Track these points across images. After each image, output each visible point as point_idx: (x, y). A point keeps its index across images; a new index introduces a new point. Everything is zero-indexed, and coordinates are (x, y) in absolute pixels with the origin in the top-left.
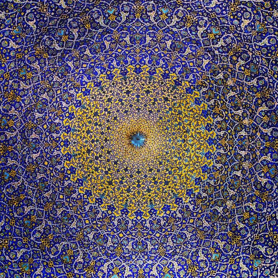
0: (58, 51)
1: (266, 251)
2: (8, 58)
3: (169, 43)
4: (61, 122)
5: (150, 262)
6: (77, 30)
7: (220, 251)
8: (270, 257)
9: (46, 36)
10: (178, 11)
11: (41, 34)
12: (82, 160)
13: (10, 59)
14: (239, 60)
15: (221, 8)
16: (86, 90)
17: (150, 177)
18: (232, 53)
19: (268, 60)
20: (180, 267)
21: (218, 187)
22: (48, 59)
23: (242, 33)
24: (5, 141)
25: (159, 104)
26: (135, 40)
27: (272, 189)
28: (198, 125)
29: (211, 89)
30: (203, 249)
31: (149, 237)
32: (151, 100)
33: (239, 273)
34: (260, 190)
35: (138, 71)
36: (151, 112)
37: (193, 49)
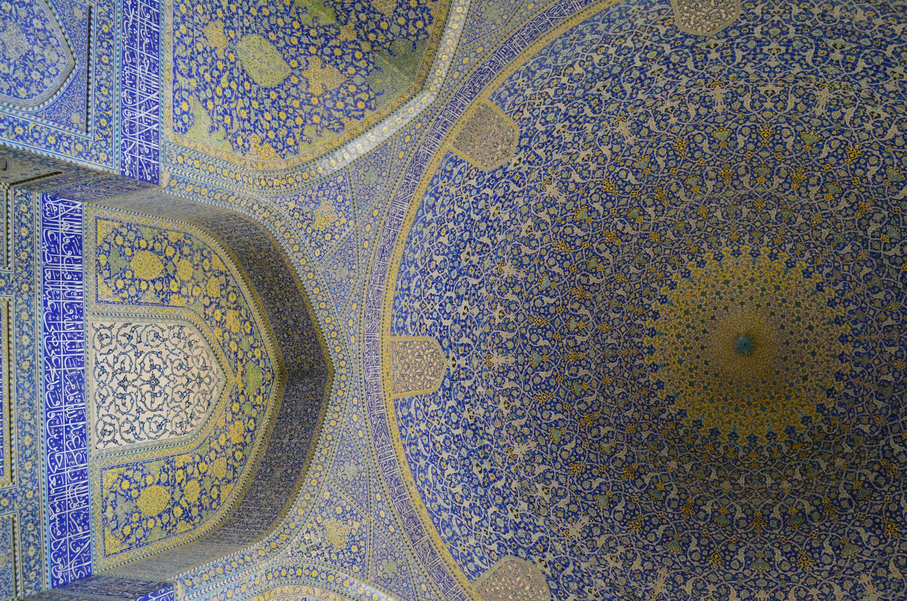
0: (865, 230)
1: (619, 511)
2: (853, 167)
3: (889, 378)
4: (765, 244)
5: (593, 367)
6: (899, 253)
8: (612, 516)
11: (889, 207)
12: (715, 274)
14: (875, 474)
16: (811, 273)
17: (698, 363)
18: (884, 463)
19: (880, 513)
21: (692, 449)
22: (854, 220)
25: (798, 369)
26: (889, 332)
27: (699, 519)
28: (773, 421)
30: (613, 433)
31: (623, 364)
32: (802, 358)
33: (589, 478)
34: (696, 504)
35: (843, 339)
36: (785, 359)
37: (884, 411)
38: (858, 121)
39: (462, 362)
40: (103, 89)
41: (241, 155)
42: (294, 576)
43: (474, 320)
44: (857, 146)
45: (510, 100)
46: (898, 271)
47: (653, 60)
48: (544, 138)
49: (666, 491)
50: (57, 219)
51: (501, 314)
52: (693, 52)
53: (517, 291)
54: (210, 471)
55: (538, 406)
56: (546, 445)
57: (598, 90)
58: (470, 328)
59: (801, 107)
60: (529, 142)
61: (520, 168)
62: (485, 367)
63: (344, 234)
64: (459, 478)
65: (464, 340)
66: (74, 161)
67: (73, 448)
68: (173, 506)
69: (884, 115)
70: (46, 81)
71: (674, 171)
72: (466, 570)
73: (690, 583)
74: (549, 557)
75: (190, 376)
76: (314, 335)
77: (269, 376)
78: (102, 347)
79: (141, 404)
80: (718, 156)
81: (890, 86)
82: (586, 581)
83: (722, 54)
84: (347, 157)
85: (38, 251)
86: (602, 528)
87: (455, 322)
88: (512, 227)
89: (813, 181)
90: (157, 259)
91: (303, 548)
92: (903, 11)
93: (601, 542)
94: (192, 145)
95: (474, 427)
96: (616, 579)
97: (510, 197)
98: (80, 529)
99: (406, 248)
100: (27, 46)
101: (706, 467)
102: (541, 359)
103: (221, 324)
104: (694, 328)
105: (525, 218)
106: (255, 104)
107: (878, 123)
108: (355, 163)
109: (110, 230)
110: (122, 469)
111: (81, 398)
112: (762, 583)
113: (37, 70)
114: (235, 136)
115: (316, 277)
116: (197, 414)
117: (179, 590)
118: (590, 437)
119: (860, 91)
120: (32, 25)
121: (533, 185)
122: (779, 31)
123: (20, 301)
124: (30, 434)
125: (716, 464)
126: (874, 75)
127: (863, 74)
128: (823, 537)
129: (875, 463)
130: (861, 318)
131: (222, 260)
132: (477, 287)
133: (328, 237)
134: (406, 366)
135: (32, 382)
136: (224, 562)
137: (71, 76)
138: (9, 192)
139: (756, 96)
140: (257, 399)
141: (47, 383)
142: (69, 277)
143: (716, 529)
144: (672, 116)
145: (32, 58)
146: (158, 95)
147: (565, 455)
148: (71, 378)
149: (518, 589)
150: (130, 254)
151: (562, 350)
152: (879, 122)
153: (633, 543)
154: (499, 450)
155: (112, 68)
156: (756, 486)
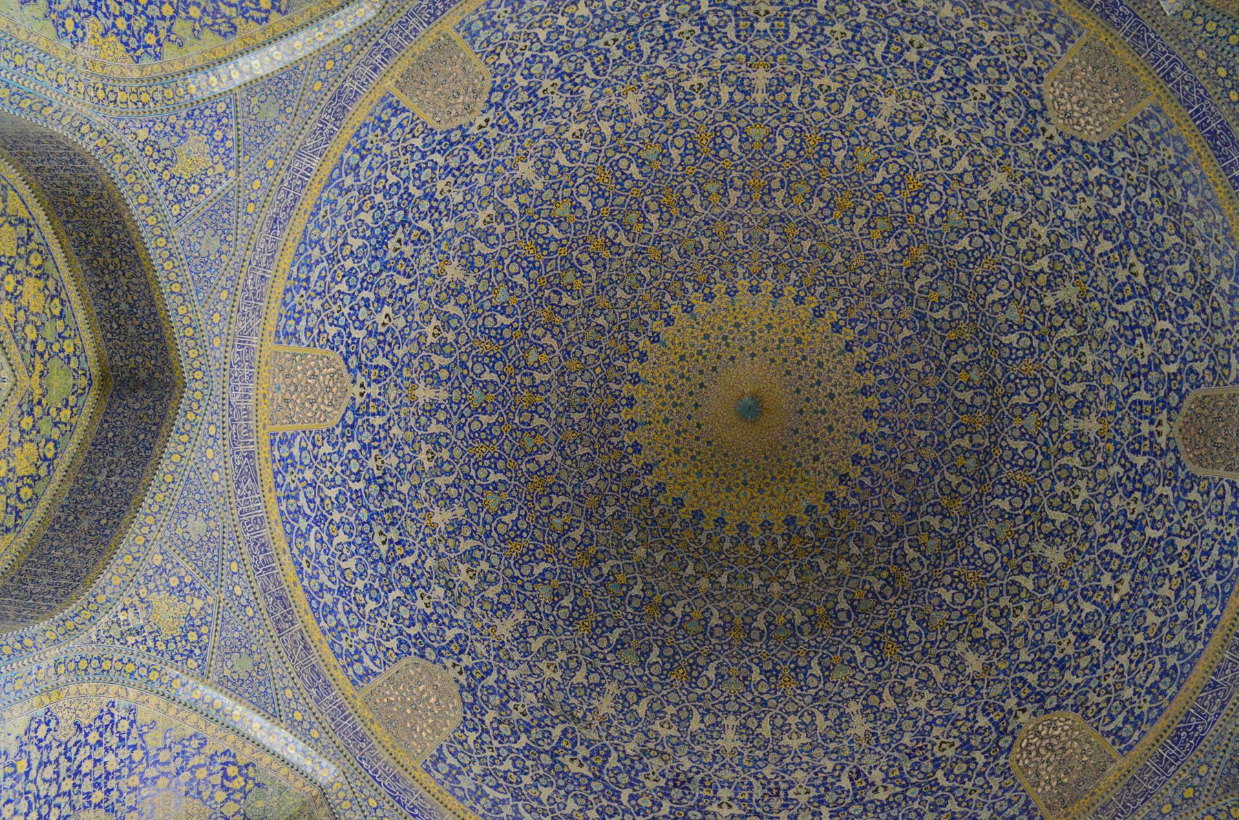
0: (912, 283)
2: (910, 201)
3: (914, 468)
4: (791, 282)
5: (553, 415)
6: (947, 317)
7: (565, 532)
9: (939, 265)
10: (969, 485)
11: (944, 258)
13: (908, 204)
14: (882, 582)
15: (972, 556)
19: (881, 630)
20: (543, 464)
23: (928, 590)
24: (770, 189)
26: (922, 411)
28: (771, 508)
29: (832, 533)
31: (593, 416)
32: (816, 433)
34: (663, 604)
35: (868, 414)
36: (796, 432)
37: (903, 508)
38: (924, 144)
39: (374, 390)
41: (69, 46)
42: (99, 671)
43: (397, 334)
44: (918, 176)
45: (484, 35)
46: (943, 338)
47: (684, 16)
48: (524, 97)
49: (628, 586)
51: (436, 331)
52: (736, 15)
53: (462, 303)
55: (473, 461)
56: (478, 514)
57: (606, 44)
58: (390, 344)
59: (860, 114)
60: (503, 99)
61: (486, 133)
62: (406, 401)
63: (219, 188)
64: (353, 548)
65: (381, 361)
69: (956, 142)
71: (690, 171)
72: (350, 672)
73: (644, 703)
74: (467, 660)
76: (159, 329)
77: (84, 382)
80: (749, 160)
81: (968, 107)
82: (512, 694)
83: (773, 25)
84: (235, 75)
86: (540, 627)
87: (370, 334)
88: (466, 213)
89: (860, 211)
91: (116, 631)
92: (997, 15)
93: (536, 645)
95: (381, 481)
96: (552, 693)
97: (468, 171)
101: (682, 558)
102: (484, 397)
104: (688, 379)
105: (485, 204)
107: (948, 151)
108: (248, 87)
112: (732, 707)
114: (63, 15)
115: (170, 246)
118: (537, 508)
119: (932, 106)
121: (501, 158)
122: (847, 9)
125: (696, 555)
126: (952, 89)
127: (939, 85)
128: (812, 654)
129: (883, 569)
130: (892, 391)
131: (23, 199)
132: (406, 289)
133: (194, 189)
134: (292, 388)
139: (806, 90)
140: (62, 414)
143: (684, 637)
144: (697, 96)
147: (502, 529)
149: (420, 701)
151: (513, 389)
152: (948, 149)
153: (579, 649)
154: (413, 516)
156: (740, 587)
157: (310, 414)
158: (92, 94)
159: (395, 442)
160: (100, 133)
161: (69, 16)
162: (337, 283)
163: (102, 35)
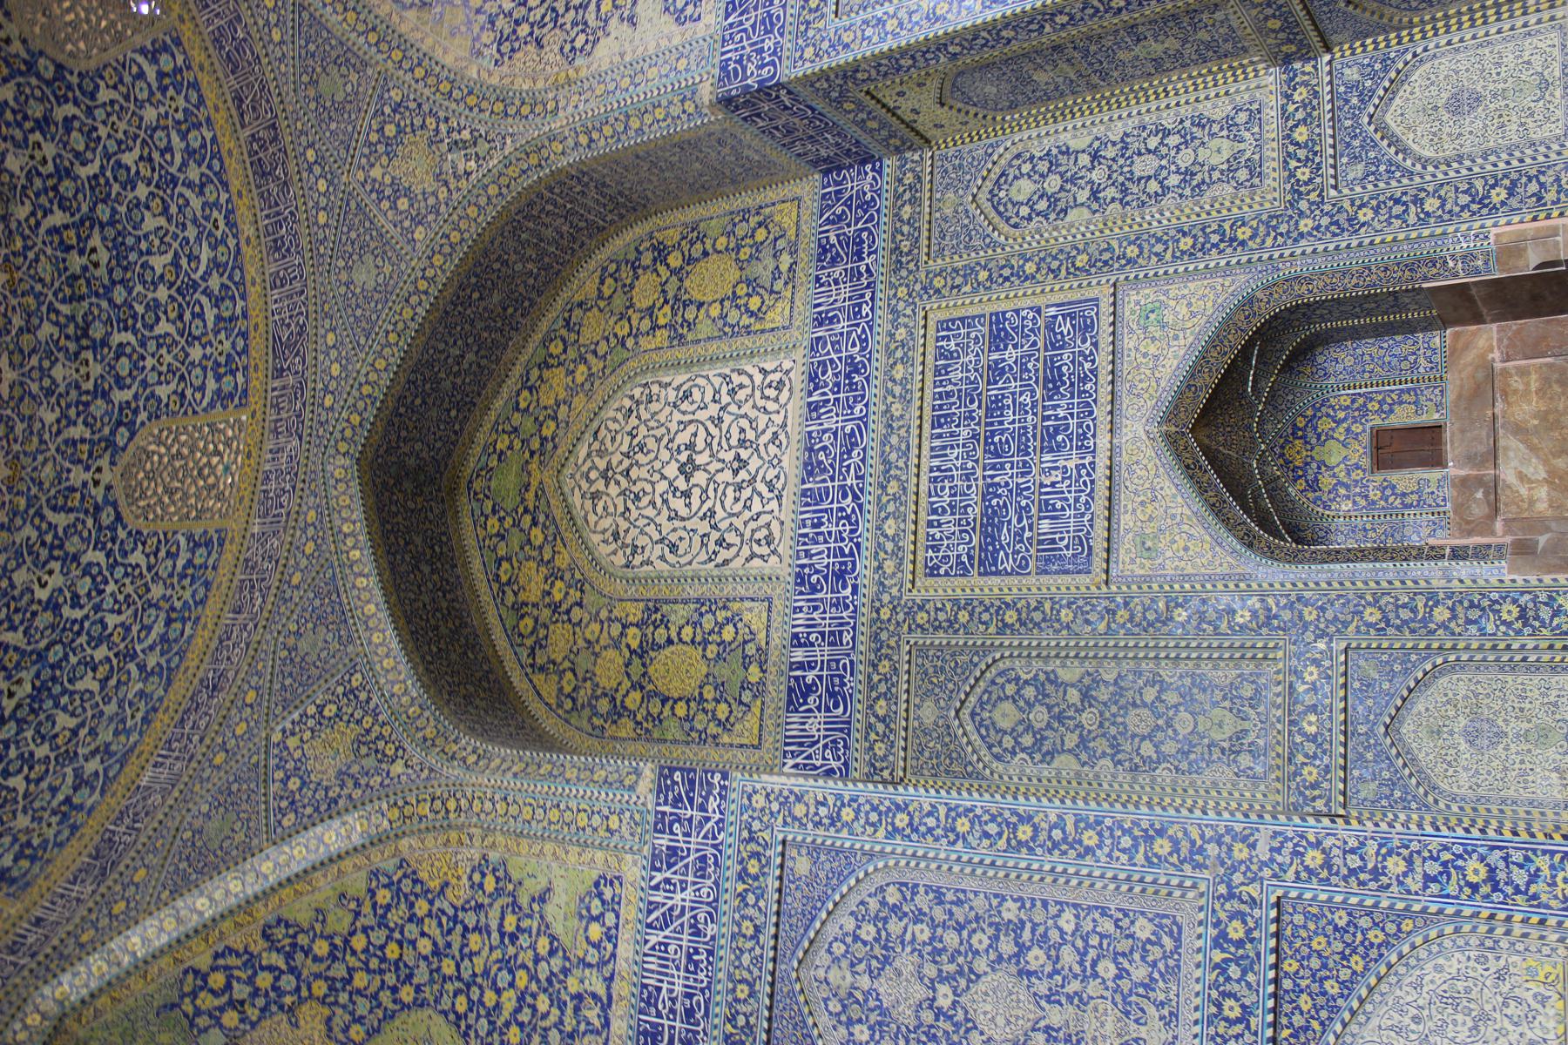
39: (78, 476)
40: (750, 932)
50: (825, 737)
54: (611, 322)
58: (43, 544)
63: (296, 716)
64: (144, 246)
65: (61, 520)
66: (811, 782)
67: (832, 361)
68: (682, 268)
70: (850, 925)
72: (180, 59)
75: (624, 483)
76: (385, 535)
77: (477, 485)
78: (768, 525)
79: (714, 431)
85: (861, 677)
87: (75, 558)
90: (659, 684)
91: (482, 147)
94: (587, 856)
95: (84, 342)
98: (833, 239)
99: (161, 699)
100: (882, 986)
103: (555, 575)
106: (448, 967)
108: (248, 851)
109: (738, 727)
110: (758, 327)
111: (810, 437)
113: (865, 943)
114: (499, 891)
116: (619, 416)
117: (706, 93)
120: (871, 1028)
123: (894, 591)
124: (894, 381)
131: (536, 694)
133: (331, 710)
135: (886, 462)
136: (623, 137)
137: (806, 944)
138: (901, 774)
140: (507, 442)
141: (863, 460)
142: (813, 637)
145: (874, 963)
146: (646, 942)
148: (825, 470)
150: (707, 688)
154: (38, 287)
155: (730, 977)
157: (183, 438)
158: (463, 802)
159: (53, 400)
160: (453, 758)
161: (490, 895)
162: (122, 624)
163: (447, 884)
